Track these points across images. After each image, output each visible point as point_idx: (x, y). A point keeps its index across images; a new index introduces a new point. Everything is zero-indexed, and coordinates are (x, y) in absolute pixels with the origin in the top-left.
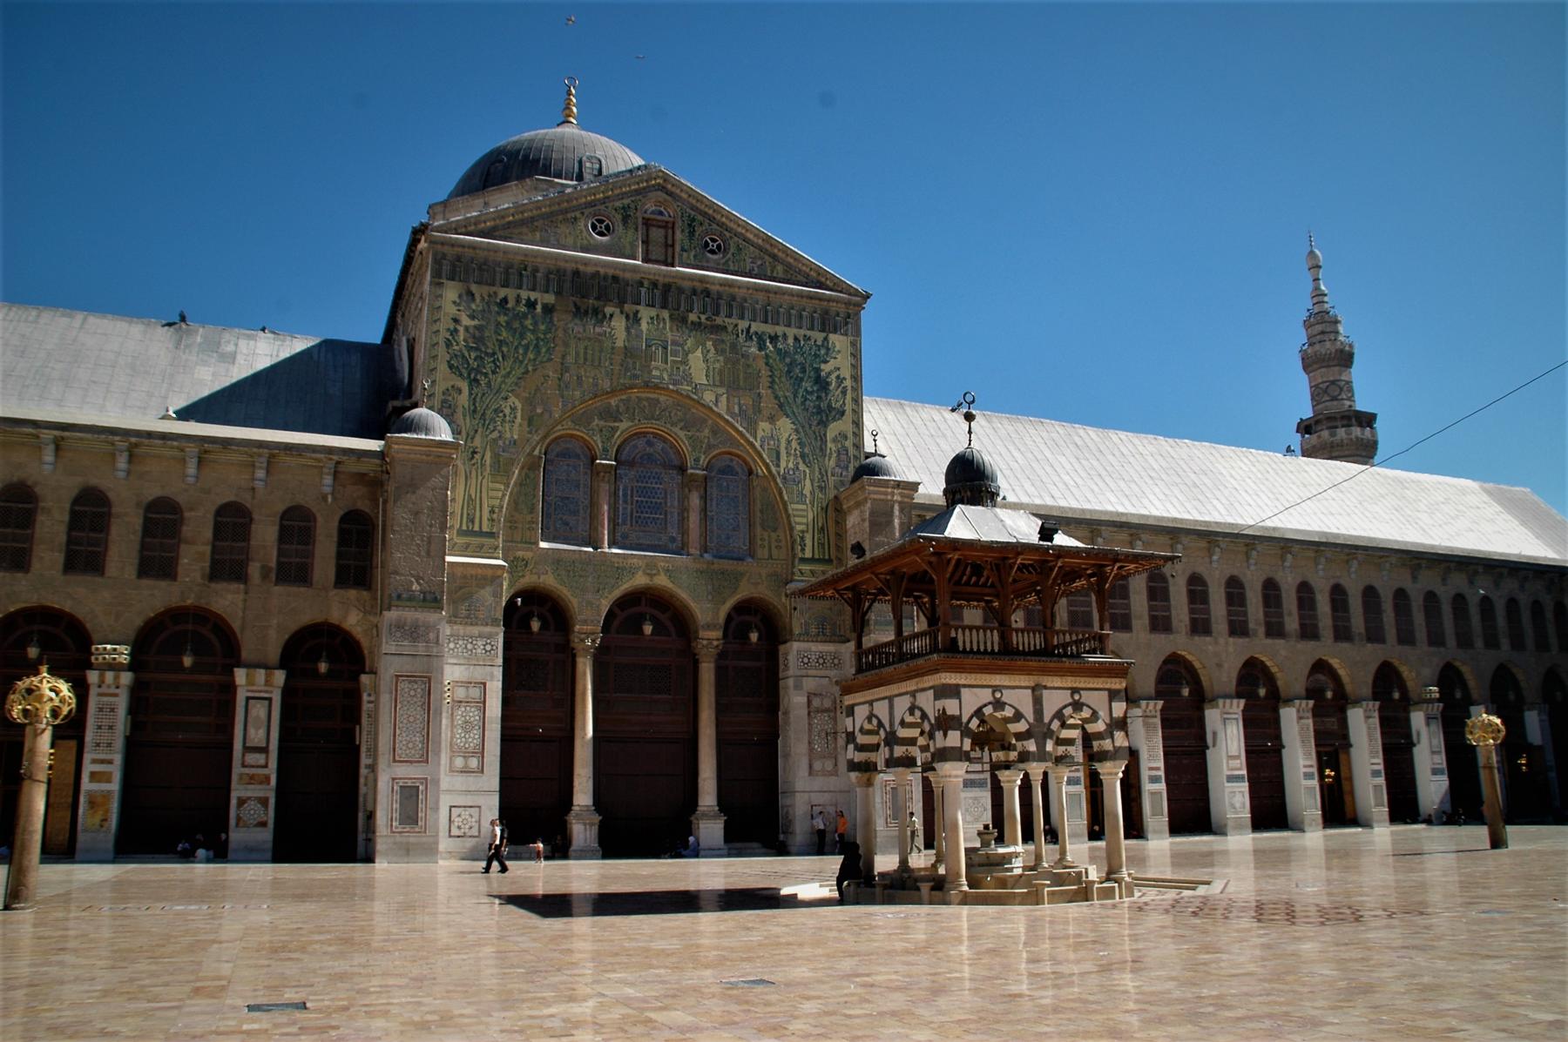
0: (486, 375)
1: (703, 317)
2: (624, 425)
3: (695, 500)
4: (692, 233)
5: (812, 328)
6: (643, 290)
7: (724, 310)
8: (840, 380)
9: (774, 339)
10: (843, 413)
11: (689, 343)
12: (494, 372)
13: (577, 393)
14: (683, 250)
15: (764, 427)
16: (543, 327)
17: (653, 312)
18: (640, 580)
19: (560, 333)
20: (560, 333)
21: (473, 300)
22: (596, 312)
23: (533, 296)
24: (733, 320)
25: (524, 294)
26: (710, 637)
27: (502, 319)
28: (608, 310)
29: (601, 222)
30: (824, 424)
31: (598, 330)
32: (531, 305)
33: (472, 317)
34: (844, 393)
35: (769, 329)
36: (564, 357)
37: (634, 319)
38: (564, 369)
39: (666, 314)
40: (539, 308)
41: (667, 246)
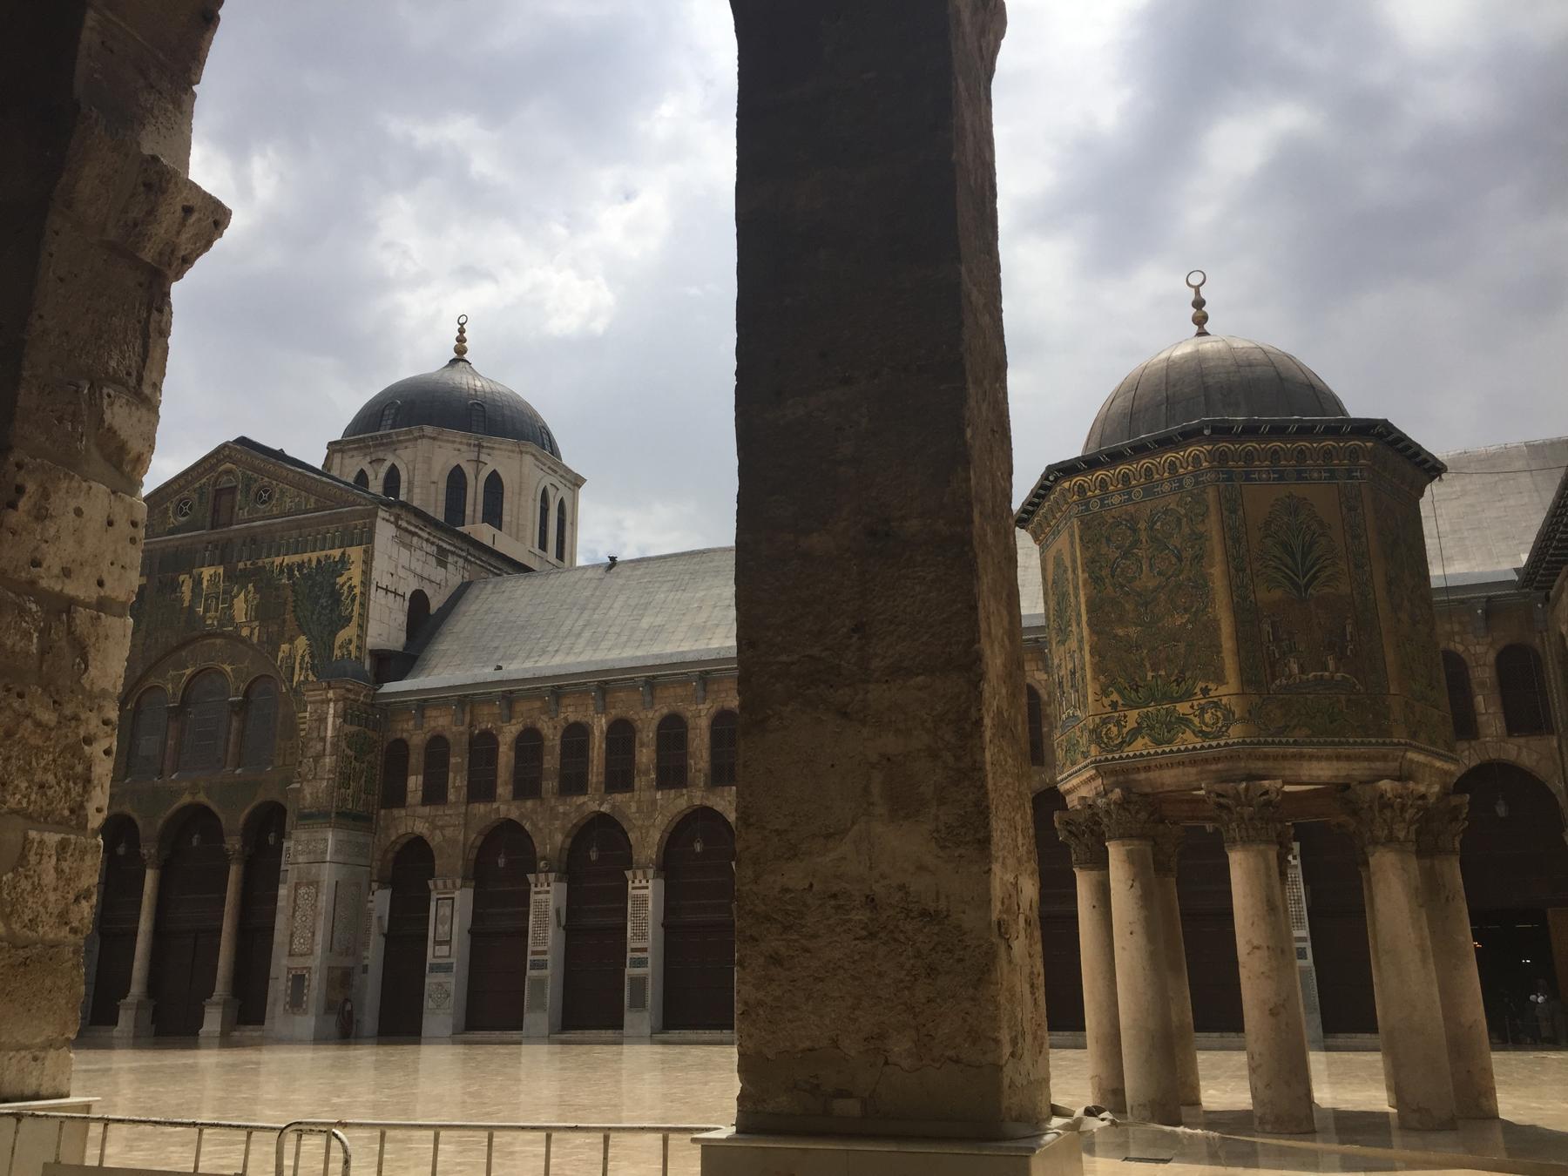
2: (188, 672)
3: (235, 724)
4: (248, 492)
8: (351, 588)
9: (301, 566)
10: (349, 619)
15: (285, 647)
17: (212, 570)
18: (186, 799)
26: (233, 843)
28: (182, 578)
30: (334, 634)
34: (353, 600)
35: (296, 558)
37: (198, 582)
39: (221, 570)
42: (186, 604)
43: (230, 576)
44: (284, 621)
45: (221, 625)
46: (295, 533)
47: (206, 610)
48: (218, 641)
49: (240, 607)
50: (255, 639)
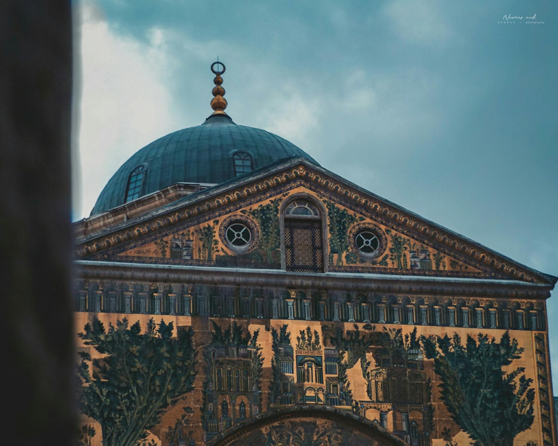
0: (121, 411)
1: (361, 326)
4: (342, 231)
5: (488, 326)
6: (290, 302)
7: (383, 317)
8: (525, 382)
9: (444, 342)
11: (346, 356)
12: (129, 408)
13: (223, 424)
14: (333, 252)
16: (180, 354)
17: (303, 325)
19: (200, 359)
20: (200, 359)
21: (102, 330)
22: (238, 330)
23: (168, 319)
24: (396, 326)
25: (157, 319)
27: (135, 349)
28: (252, 328)
29: (238, 228)
31: (242, 351)
32: (166, 329)
33: (101, 350)
35: (437, 331)
36: (206, 385)
37: (281, 339)
38: (208, 398)
39: (317, 327)
40: (175, 333)
41: (314, 248)
42: (267, 364)
43: (335, 337)
44: (431, 409)
45: (330, 401)
46: (427, 299)
47: (302, 377)
48: (320, 422)
49: (359, 381)
50: (389, 426)
